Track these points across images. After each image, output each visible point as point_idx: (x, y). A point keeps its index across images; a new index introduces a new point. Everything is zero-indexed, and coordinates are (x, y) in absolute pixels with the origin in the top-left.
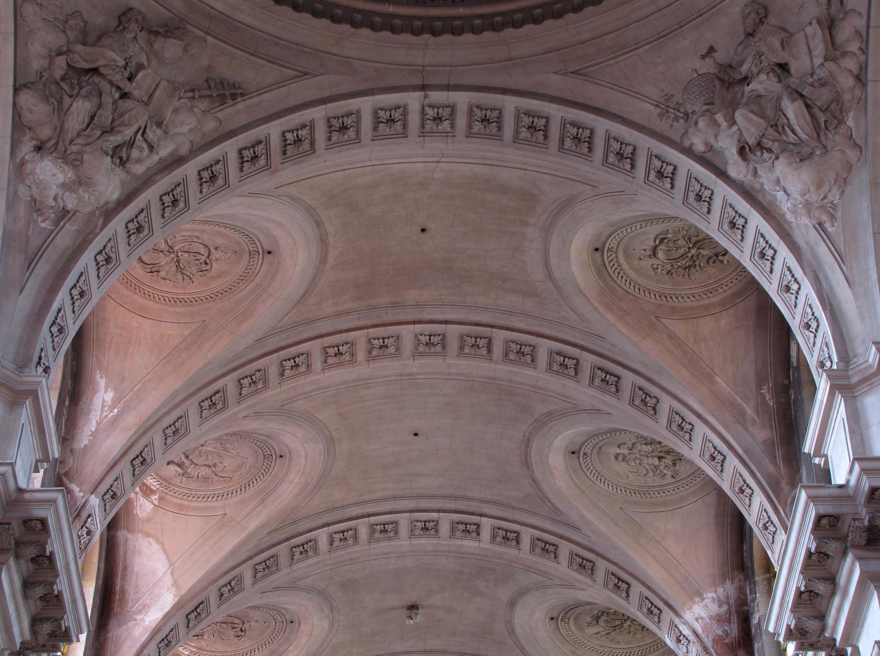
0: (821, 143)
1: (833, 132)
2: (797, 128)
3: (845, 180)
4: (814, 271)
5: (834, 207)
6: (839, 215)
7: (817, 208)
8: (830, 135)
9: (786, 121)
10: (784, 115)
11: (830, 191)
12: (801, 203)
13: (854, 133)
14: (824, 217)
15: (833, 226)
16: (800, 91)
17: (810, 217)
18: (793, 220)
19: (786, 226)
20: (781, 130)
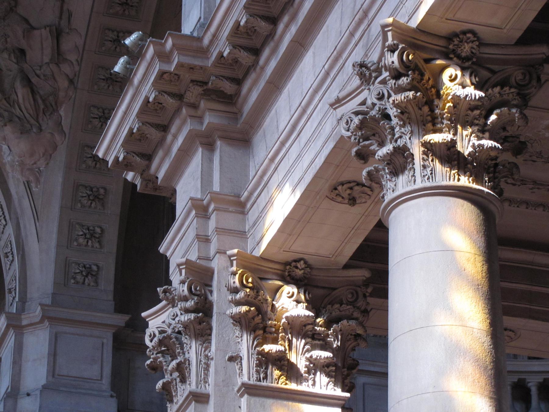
0: (38, 122)
1: (48, 117)
2: (22, 106)
3: (51, 155)
4: (18, 218)
5: (40, 172)
6: (42, 180)
7: (28, 169)
8: (45, 119)
9: (16, 98)
10: (16, 93)
11: (39, 160)
12: (18, 161)
13: (63, 121)
14: (31, 178)
15: (37, 187)
16: (30, 77)
17: (22, 175)
18: (10, 171)
19: (5, 174)
20: (12, 104)
